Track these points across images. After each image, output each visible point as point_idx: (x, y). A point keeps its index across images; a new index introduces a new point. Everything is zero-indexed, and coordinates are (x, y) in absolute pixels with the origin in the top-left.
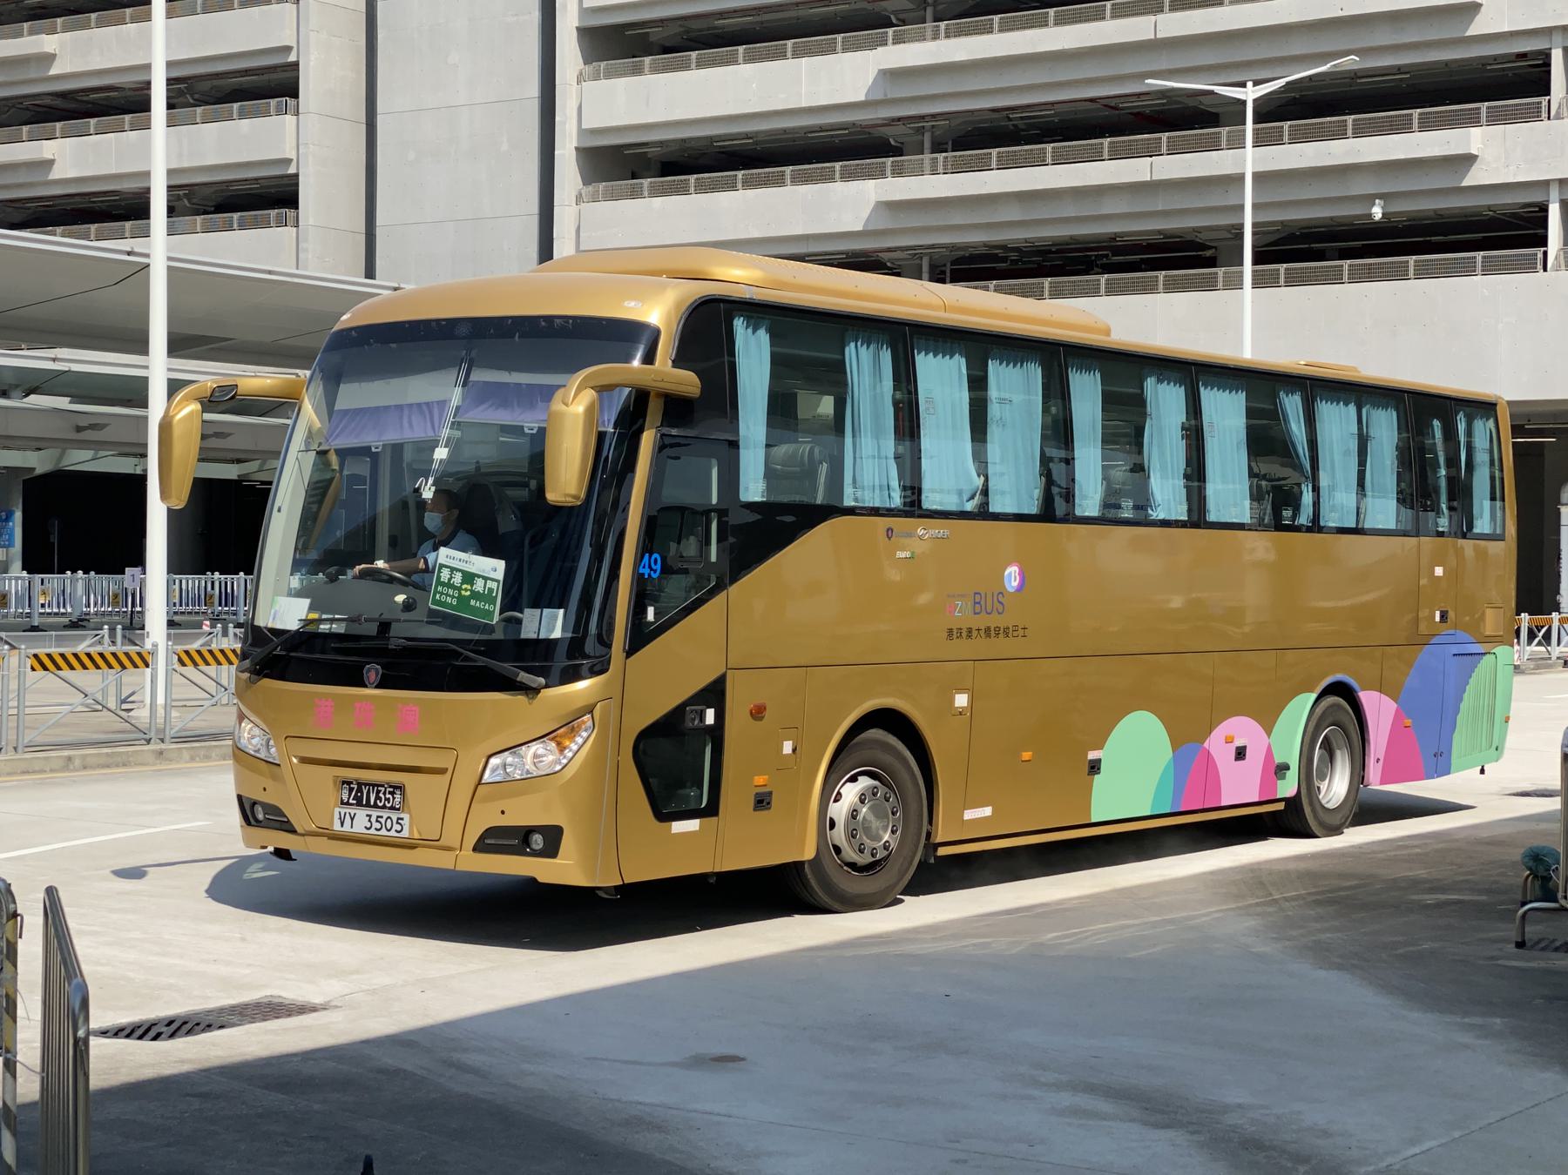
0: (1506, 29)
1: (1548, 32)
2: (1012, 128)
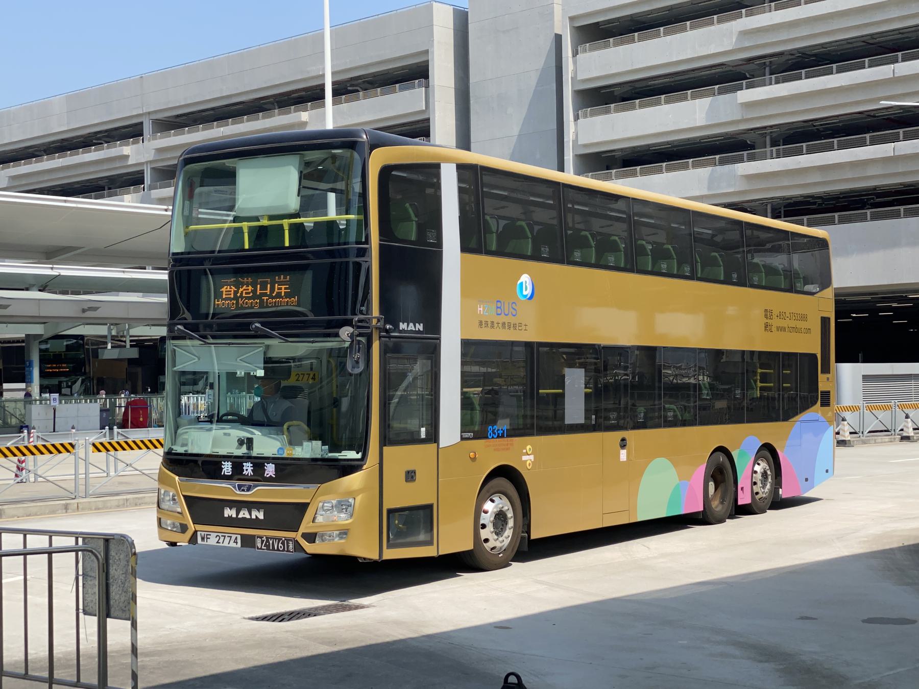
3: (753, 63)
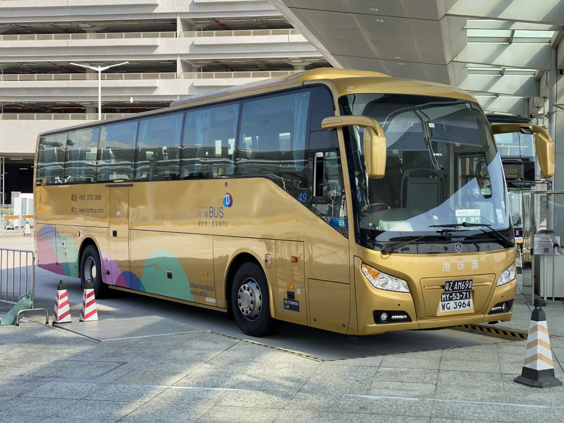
0: (165, 53)
1: (176, 55)
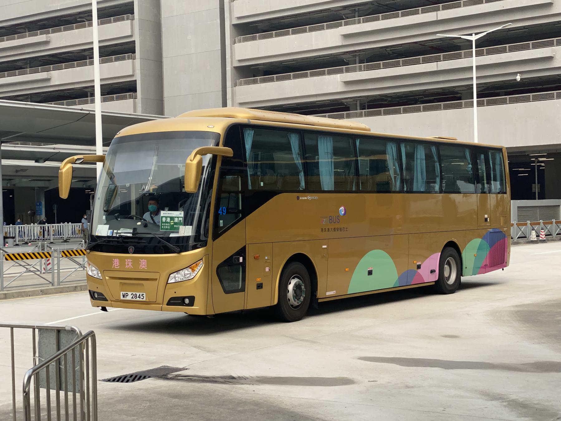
2: (387, 54)
3: (348, 9)
